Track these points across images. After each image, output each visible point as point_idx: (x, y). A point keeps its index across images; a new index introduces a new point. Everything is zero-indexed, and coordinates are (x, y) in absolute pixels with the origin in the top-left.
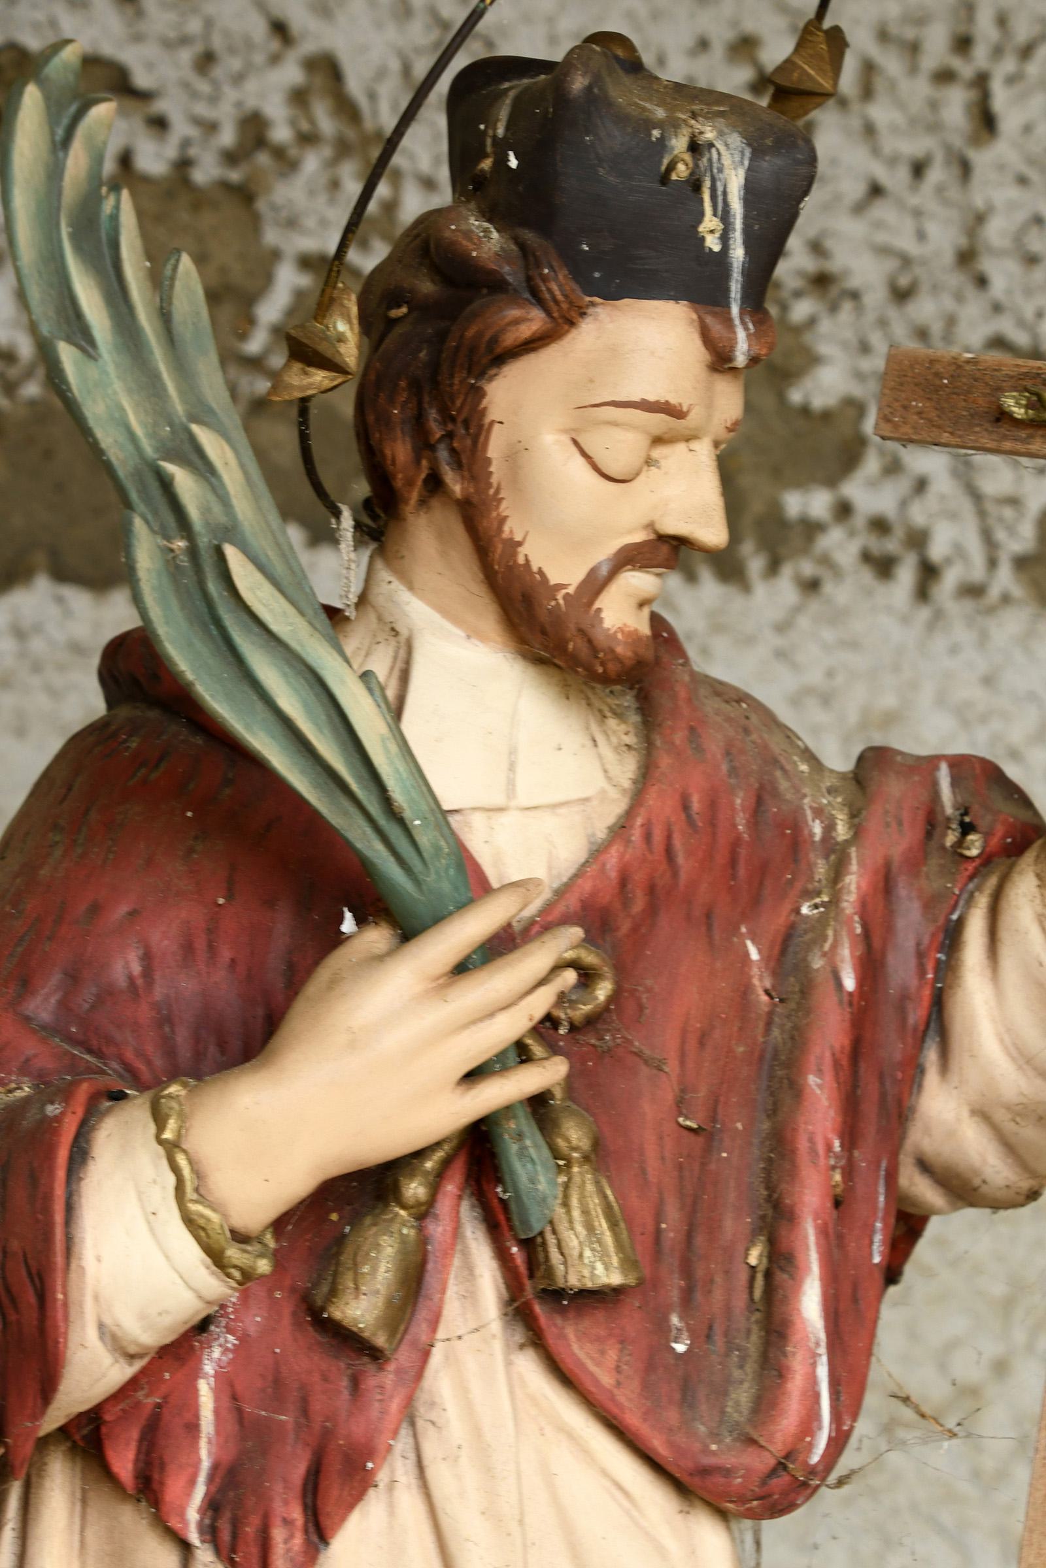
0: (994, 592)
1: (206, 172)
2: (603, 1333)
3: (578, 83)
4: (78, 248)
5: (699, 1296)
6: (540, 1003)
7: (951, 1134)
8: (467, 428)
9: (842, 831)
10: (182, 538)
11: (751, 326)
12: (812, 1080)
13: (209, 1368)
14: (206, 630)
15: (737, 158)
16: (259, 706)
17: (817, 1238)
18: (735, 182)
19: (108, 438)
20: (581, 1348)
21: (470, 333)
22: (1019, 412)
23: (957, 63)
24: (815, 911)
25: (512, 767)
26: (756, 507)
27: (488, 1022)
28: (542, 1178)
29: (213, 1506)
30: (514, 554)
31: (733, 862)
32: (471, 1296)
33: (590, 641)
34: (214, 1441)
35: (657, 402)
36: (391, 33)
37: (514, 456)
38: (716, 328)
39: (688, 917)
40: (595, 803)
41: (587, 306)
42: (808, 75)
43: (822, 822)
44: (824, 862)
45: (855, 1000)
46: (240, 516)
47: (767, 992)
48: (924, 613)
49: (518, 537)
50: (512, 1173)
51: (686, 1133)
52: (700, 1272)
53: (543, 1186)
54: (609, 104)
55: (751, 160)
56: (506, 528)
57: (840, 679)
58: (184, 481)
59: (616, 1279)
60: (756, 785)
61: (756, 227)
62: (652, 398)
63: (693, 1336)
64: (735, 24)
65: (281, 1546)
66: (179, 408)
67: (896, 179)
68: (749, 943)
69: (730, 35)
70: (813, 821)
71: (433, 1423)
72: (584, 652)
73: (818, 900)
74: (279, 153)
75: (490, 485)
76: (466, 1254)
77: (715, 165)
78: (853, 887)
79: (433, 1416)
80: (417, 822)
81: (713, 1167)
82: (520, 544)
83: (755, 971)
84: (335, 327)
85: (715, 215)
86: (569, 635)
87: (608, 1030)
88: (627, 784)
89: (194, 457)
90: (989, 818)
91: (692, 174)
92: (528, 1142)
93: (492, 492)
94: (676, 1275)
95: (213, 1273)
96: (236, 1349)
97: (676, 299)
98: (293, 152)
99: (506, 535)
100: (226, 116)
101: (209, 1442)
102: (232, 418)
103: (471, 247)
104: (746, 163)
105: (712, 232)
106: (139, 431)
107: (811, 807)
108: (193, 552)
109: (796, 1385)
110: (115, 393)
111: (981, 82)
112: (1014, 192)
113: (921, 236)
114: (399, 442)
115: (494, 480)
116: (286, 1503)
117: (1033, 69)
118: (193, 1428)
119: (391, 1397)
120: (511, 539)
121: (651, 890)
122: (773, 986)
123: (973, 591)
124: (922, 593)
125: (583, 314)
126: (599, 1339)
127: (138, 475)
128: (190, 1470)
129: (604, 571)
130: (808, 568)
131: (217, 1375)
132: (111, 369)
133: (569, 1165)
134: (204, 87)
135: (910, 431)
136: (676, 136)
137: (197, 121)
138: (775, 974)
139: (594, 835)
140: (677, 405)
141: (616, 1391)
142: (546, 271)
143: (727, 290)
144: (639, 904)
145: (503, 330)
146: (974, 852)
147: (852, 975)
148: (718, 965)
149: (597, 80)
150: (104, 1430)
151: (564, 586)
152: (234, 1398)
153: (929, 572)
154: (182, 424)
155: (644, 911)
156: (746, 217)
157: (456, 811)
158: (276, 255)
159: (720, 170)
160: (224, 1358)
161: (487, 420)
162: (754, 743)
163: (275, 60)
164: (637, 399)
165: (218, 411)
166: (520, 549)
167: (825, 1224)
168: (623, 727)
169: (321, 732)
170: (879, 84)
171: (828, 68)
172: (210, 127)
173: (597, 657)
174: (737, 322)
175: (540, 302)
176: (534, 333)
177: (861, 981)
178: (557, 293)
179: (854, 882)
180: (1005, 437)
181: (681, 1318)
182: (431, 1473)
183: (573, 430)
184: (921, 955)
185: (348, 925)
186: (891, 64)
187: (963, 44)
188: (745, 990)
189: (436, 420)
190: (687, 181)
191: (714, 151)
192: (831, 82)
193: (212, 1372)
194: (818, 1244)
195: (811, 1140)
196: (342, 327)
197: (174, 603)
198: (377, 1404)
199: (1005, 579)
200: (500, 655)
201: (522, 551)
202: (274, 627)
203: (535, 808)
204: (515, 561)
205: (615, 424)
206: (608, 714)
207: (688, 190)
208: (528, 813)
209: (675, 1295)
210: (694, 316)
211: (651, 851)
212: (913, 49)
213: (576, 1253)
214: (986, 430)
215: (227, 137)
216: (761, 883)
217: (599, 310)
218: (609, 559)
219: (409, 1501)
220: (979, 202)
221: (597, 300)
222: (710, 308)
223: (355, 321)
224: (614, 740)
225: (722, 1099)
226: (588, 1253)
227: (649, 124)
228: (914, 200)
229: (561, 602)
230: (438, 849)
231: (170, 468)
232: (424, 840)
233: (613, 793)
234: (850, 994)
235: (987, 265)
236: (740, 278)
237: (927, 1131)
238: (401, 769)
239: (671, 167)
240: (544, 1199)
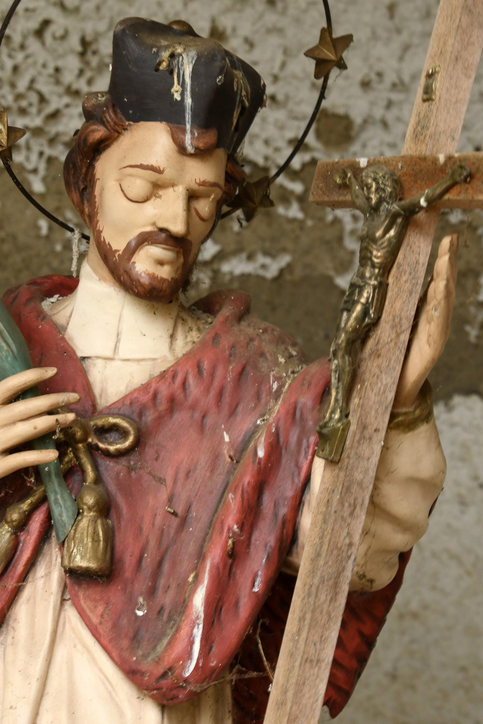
2: (98, 597)
5: (160, 592)
11: (196, 134)
20: (85, 603)
22: (338, 180)
25: (118, 341)
28: (64, 515)
30: (100, 237)
32: (48, 575)
33: (130, 276)
37: (101, 195)
40: (159, 361)
41: (128, 126)
43: (278, 383)
44: (274, 401)
45: (262, 462)
47: (231, 457)
49: (101, 229)
53: (65, 518)
56: (98, 225)
60: (244, 362)
62: (145, 163)
68: (225, 433)
70: (274, 382)
72: (128, 282)
73: (265, 418)
78: (276, 411)
81: (183, 534)
82: (101, 232)
86: (120, 273)
88: (180, 355)
92: (59, 497)
97: (161, 121)
99: (97, 228)
109: (184, 632)
114: (74, 192)
115: (97, 205)
120: (99, 230)
122: (235, 455)
125: (125, 129)
126: (95, 600)
129: (133, 244)
133: (83, 512)
138: (236, 451)
140: (158, 167)
143: (184, 117)
144: (163, 406)
147: (263, 450)
155: (167, 410)
161: (95, 179)
164: (139, 164)
168: (198, 335)
171: (332, 48)
173: (133, 284)
176: (101, 137)
178: (108, 118)
180: (340, 195)
192: (335, 55)
194: (211, 571)
195: (222, 523)
201: (103, 234)
203: (128, 360)
204: (101, 240)
205: (131, 175)
209: (144, 588)
210: (169, 129)
211: (174, 382)
216: (237, 406)
218: (134, 238)
221: (131, 123)
222: (176, 125)
224: (189, 339)
226: (75, 551)
234: (260, 459)
236: (190, 112)
240: (65, 525)
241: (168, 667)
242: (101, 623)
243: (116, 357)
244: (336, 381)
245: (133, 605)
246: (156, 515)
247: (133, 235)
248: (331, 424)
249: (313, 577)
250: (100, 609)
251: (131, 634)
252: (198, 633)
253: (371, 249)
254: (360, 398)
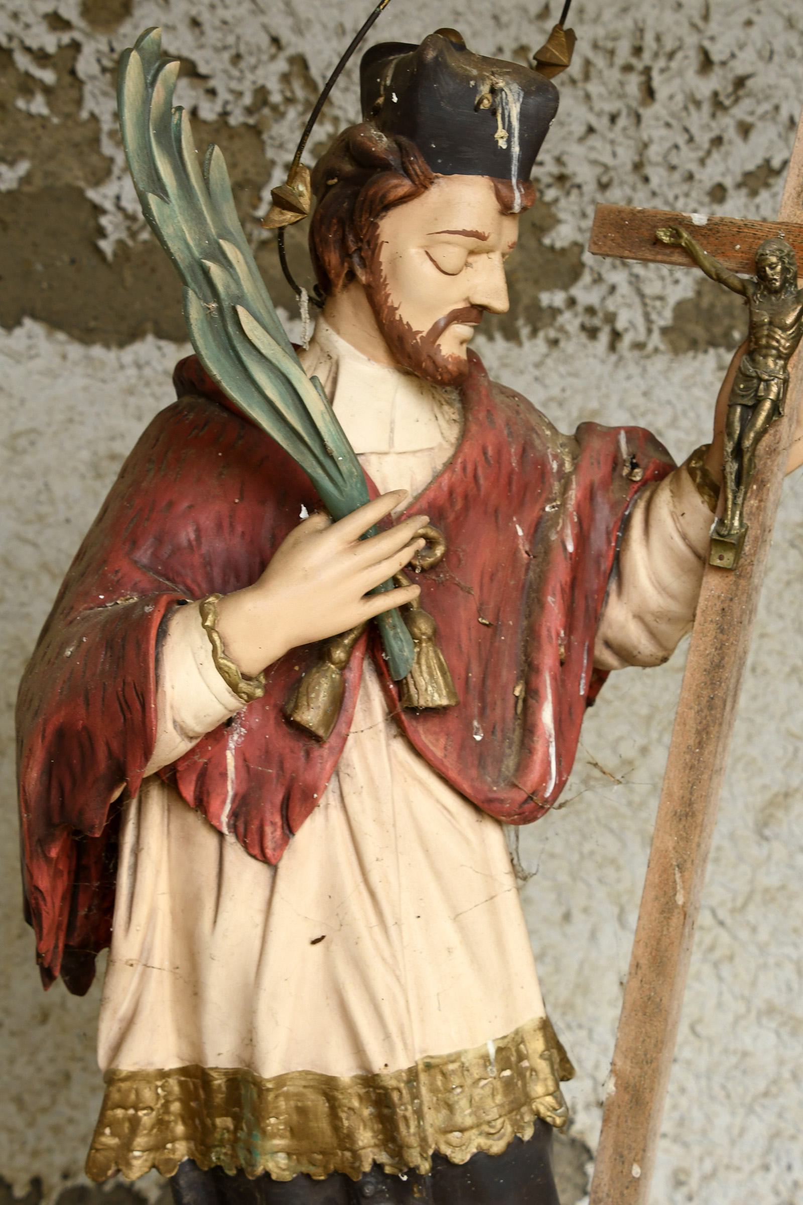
0: (650, 347)
1: (236, 118)
2: (437, 730)
3: (431, 55)
4: (159, 142)
5: (488, 711)
6: (406, 556)
7: (623, 628)
8: (369, 245)
9: (568, 467)
10: (214, 302)
11: (522, 190)
12: (550, 599)
13: (232, 745)
14: (226, 351)
15: (516, 97)
16: (256, 394)
17: (551, 682)
18: (514, 110)
19: (174, 247)
20: (426, 737)
21: (371, 192)
22: (666, 239)
23: (634, 61)
24: (553, 510)
25: (392, 431)
26: (525, 300)
27: (378, 566)
28: (406, 649)
29: (234, 815)
30: (394, 315)
31: (510, 483)
32: (368, 711)
33: (434, 362)
34: (235, 782)
35: (472, 231)
36: (335, 43)
37: (395, 260)
38: (504, 191)
39: (485, 512)
40: (436, 450)
41: (434, 178)
42: (555, 55)
45: (573, 556)
46: (246, 291)
47: (527, 552)
48: (613, 358)
49: (396, 305)
50: (390, 646)
51: (482, 626)
52: (489, 699)
53: (406, 653)
54: (447, 66)
55: (524, 98)
56: (390, 300)
57: (568, 393)
58: (215, 270)
59: (445, 702)
60: (523, 442)
61: (526, 135)
62: (468, 229)
63: (485, 732)
64: (516, 39)
65: (270, 835)
66: (213, 231)
67: (601, 124)
68: (518, 527)
69: (514, 45)
71: (348, 775)
72: (431, 368)
73: (554, 504)
74: (275, 108)
75: (381, 277)
76: (366, 688)
77: (504, 101)
78: (573, 497)
79: (349, 771)
80: (340, 458)
81: (497, 644)
82: (397, 309)
83: (520, 541)
84: (298, 188)
85: (504, 128)
86: (423, 359)
87: (442, 572)
88: (453, 440)
89: (221, 258)
90: (646, 461)
91: (492, 106)
92: (399, 630)
93: (382, 280)
94: (476, 701)
95: (232, 696)
96: (246, 735)
97: (482, 174)
98: (282, 108)
99: (389, 304)
100: (247, 87)
101: (232, 782)
102: (241, 238)
103: (372, 145)
104: (521, 100)
105: (502, 138)
106: (191, 243)
107: (552, 454)
108: (220, 309)
110: (179, 222)
111: (647, 71)
112: (663, 132)
113: (614, 155)
114: (333, 253)
115: (383, 274)
116: (272, 814)
117: (674, 65)
118: (224, 775)
119: (327, 761)
120: (392, 306)
121: (466, 497)
122: (530, 550)
123: (639, 346)
124: (612, 347)
125: (432, 183)
126: (435, 733)
127: (191, 267)
128: (223, 796)
129: (442, 324)
130: (552, 334)
131: (236, 749)
132: (176, 208)
133: (420, 643)
134: (235, 73)
135: (608, 250)
136: (483, 85)
137: (232, 91)
139: (435, 468)
141: (444, 760)
142: (412, 158)
143: (510, 170)
144: (459, 505)
145: (389, 191)
146: (638, 478)
148: (501, 538)
149: (440, 53)
150: (178, 775)
151: (421, 332)
152: (245, 760)
153: (616, 336)
154: (214, 239)
156: (520, 130)
157: (362, 454)
158: (273, 163)
159: (507, 104)
160: (239, 740)
161: (380, 241)
162: (521, 419)
163: (273, 58)
164: (460, 229)
165: (234, 233)
166: (397, 312)
167: (555, 674)
168: (452, 410)
169: (289, 409)
170: (593, 73)
172: (239, 94)
173: (438, 371)
174: (515, 187)
175: (408, 175)
177: (577, 547)
179: (574, 494)
180: (658, 253)
181: (479, 723)
182: (348, 800)
183: (427, 246)
184: (608, 533)
185: (304, 514)
186: (600, 62)
187: (638, 51)
188: (515, 551)
189: (352, 241)
190: (489, 110)
191: (503, 93)
193: (233, 747)
194: (551, 685)
195: (549, 631)
196: (301, 188)
197: (210, 338)
198: (319, 765)
199: (656, 339)
200: (386, 370)
201: (398, 312)
202: (263, 351)
203: (404, 453)
204: (394, 318)
205: (448, 243)
206: (444, 403)
207: (489, 115)
208: (400, 455)
209: (476, 711)
210: (492, 184)
212: (612, 53)
213: (424, 688)
214: (648, 249)
215: (247, 100)
216: (524, 494)
217: (440, 180)
218: (444, 318)
219: (336, 814)
220: (645, 137)
221: (440, 175)
222: (500, 180)
223: (309, 185)
224: (447, 417)
225: (502, 609)
226: (430, 688)
227: (469, 78)
228: (611, 136)
229: (419, 340)
230: (351, 473)
231: (208, 263)
232: (344, 468)
233: (446, 445)
234: (571, 554)
235: (649, 171)
237: (610, 626)
238: (332, 429)
239: (480, 102)
240: (407, 660)
241: (531, 792)
242: (446, 756)
243: (392, 450)
244: (733, 484)
245: (469, 729)
246: (470, 629)
247: (442, 313)
248: (733, 532)
249: (713, 690)
250: (442, 741)
251: (476, 762)
252: (552, 750)
253: (778, 337)
254: (761, 501)
